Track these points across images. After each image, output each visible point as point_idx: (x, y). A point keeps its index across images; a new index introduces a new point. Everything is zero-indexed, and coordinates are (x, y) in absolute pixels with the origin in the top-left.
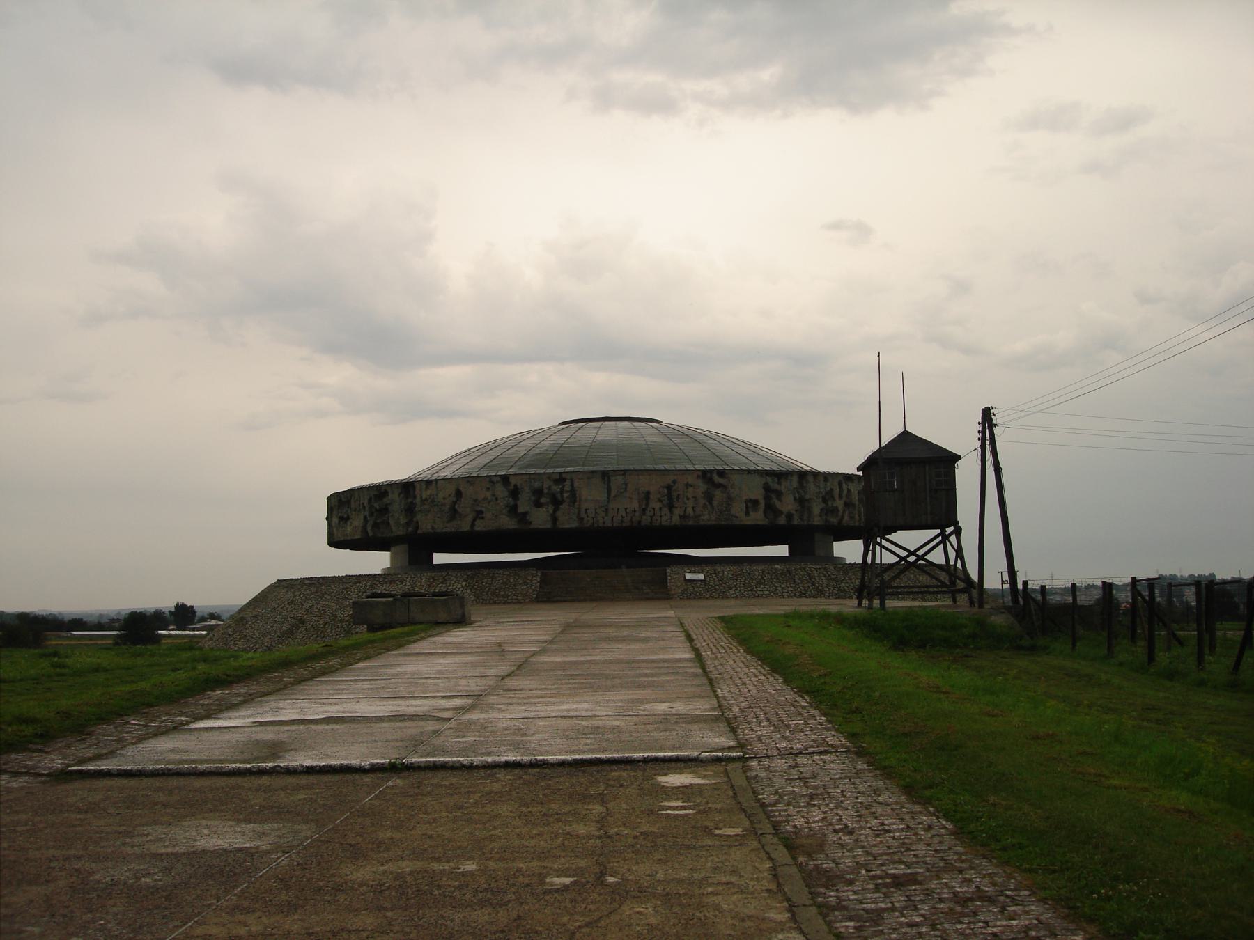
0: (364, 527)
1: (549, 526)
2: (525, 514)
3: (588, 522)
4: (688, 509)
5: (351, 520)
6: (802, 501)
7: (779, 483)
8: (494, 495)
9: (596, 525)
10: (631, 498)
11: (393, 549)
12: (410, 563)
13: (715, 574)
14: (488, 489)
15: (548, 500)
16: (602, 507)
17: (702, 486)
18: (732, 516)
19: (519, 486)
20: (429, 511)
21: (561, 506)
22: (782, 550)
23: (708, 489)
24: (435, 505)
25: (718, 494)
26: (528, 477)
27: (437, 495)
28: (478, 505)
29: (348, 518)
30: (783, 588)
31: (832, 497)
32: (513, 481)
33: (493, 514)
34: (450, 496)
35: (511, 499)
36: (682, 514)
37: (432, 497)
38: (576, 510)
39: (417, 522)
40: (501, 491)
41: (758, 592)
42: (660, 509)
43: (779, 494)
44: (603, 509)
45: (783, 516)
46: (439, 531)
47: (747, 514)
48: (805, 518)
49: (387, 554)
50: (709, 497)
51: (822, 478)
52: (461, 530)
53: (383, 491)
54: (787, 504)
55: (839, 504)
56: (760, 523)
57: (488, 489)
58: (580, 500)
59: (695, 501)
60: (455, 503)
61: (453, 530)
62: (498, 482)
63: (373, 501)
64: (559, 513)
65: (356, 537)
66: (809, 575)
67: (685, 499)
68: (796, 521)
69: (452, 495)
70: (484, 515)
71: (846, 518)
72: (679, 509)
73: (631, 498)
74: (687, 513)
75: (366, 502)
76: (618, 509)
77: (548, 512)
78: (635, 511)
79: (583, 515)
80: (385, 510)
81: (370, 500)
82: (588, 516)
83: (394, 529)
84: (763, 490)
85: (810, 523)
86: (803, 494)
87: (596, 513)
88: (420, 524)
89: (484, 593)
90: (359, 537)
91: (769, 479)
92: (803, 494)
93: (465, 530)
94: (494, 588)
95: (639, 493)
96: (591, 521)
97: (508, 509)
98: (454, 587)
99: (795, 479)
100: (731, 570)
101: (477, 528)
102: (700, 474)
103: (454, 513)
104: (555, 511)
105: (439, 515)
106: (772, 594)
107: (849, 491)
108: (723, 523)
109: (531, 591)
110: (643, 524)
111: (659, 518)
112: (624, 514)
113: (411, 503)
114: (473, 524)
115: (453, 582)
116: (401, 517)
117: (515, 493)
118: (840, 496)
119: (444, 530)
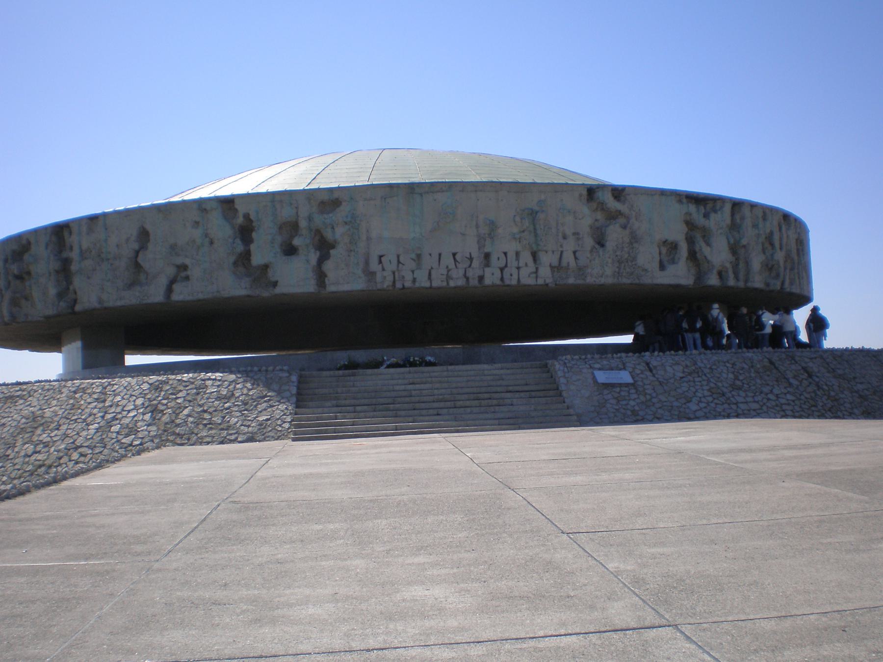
2: (266, 267)
3: (384, 281)
4: (565, 255)
6: (734, 249)
7: (706, 216)
8: (206, 235)
10: (463, 235)
13: (651, 370)
14: (197, 223)
17: (587, 217)
19: (252, 217)
20: (94, 270)
21: (332, 252)
27: (106, 241)
30: (777, 396)
31: (772, 245)
32: (241, 209)
34: (128, 240)
35: (238, 241)
36: (555, 263)
41: (741, 405)
42: (517, 254)
44: (413, 256)
45: (715, 272)
46: (111, 304)
47: (662, 267)
48: (742, 275)
49: (61, 354)
51: (760, 214)
52: (149, 301)
53: (24, 242)
55: (780, 256)
56: (683, 282)
57: (197, 224)
58: (369, 239)
59: (578, 239)
64: (328, 266)
66: (805, 369)
68: (731, 282)
70: (189, 273)
73: (463, 235)
76: (440, 255)
77: (308, 261)
78: (471, 259)
79: (374, 266)
82: (383, 270)
84: (684, 225)
85: (749, 284)
87: (399, 262)
91: (692, 208)
95: (477, 226)
96: (390, 278)
99: (728, 208)
100: (677, 364)
101: (176, 297)
102: (585, 193)
104: (321, 260)
106: (765, 408)
107: (788, 236)
110: (488, 281)
111: (515, 272)
112: (452, 265)
114: (169, 290)
118: (781, 249)
119: (119, 303)
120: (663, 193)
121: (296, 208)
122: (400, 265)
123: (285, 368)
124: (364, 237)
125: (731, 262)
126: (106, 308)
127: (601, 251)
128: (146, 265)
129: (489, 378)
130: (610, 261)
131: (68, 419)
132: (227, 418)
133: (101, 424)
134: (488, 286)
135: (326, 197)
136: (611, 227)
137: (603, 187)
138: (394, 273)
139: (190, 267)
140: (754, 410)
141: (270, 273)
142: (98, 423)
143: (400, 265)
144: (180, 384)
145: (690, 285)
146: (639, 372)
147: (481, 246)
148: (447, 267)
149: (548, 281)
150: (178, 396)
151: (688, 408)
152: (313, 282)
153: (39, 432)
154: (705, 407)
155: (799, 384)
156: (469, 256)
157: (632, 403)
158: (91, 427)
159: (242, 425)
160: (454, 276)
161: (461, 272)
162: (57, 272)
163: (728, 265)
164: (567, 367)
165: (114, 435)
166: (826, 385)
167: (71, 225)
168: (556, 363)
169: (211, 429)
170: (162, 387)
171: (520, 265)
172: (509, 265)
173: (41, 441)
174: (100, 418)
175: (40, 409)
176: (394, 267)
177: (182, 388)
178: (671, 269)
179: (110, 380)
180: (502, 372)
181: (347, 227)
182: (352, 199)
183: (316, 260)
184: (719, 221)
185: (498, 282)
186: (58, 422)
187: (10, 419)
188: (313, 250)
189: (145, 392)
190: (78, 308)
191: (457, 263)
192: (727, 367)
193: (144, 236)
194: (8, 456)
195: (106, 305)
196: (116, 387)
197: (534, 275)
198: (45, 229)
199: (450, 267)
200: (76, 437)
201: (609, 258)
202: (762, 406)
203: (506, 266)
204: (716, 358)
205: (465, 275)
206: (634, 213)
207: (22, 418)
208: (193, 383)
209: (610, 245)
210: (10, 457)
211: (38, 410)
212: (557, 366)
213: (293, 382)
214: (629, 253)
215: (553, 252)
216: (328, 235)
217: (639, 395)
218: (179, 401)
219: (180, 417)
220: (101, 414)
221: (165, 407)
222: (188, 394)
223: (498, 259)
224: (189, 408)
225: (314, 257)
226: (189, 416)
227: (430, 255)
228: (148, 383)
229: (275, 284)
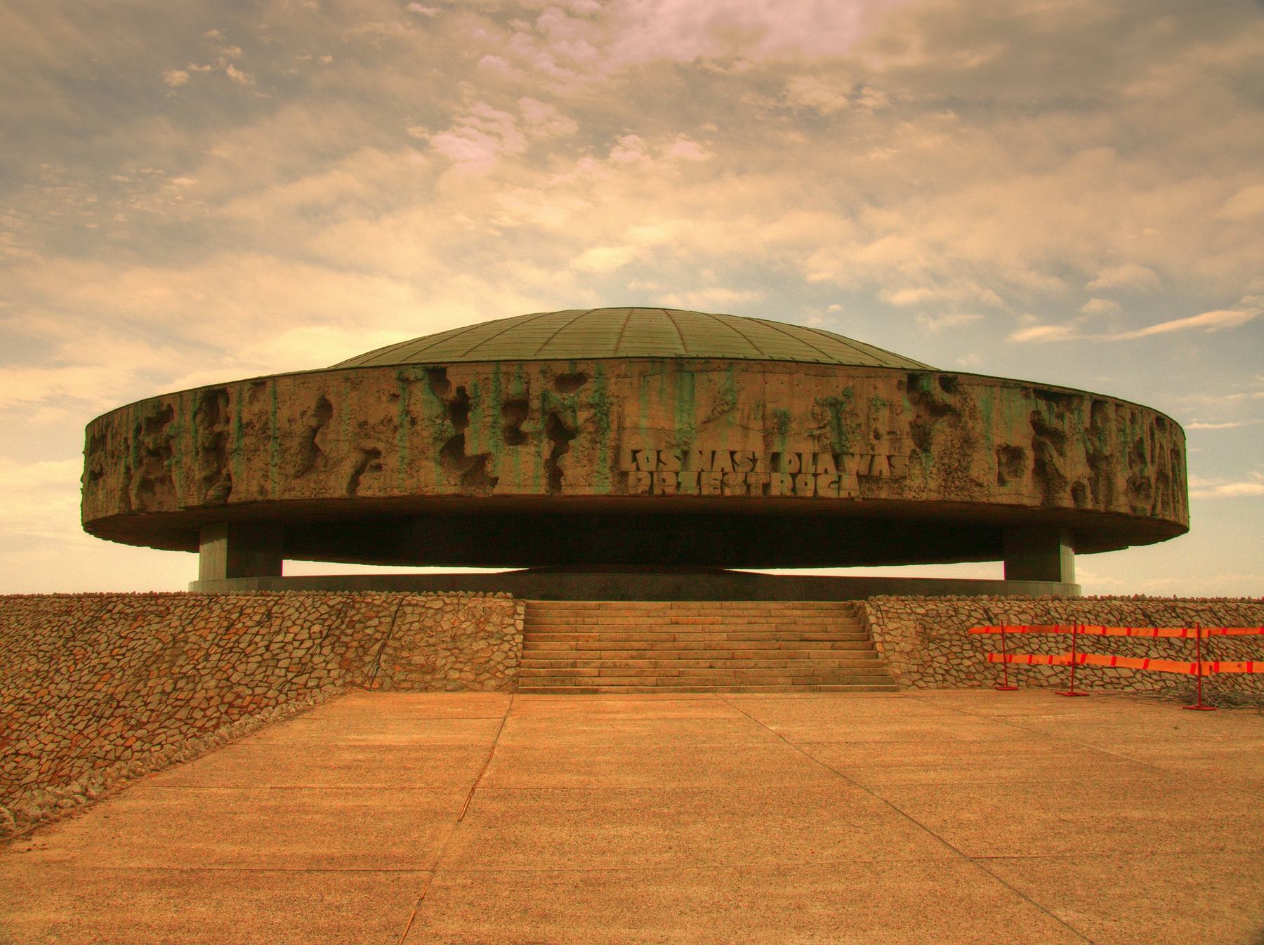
0: (125, 489)
1: (539, 488)
2: (482, 459)
3: (638, 484)
4: (877, 459)
5: (104, 477)
6: (1093, 460)
7: (1060, 417)
8: (408, 413)
9: (657, 491)
11: (201, 547)
12: (231, 573)
15: (540, 426)
16: (672, 446)
17: (908, 414)
18: (972, 480)
19: (468, 393)
20: (257, 450)
21: (571, 442)
22: (993, 570)
23: (918, 416)
24: (269, 437)
25: (942, 432)
26: (492, 368)
28: (368, 436)
29: (101, 474)
32: (455, 379)
33: (403, 458)
34: (304, 413)
35: (448, 422)
37: (264, 418)
38: (610, 454)
39: (229, 477)
40: (425, 403)
42: (815, 456)
43: (1058, 438)
44: (678, 453)
45: (1068, 489)
46: (275, 496)
47: (1002, 481)
49: (197, 556)
50: (923, 440)
51: (1128, 417)
53: (164, 408)
54: (1073, 466)
55: (1151, 471)
56: (1026, 501)
57: (395, 397)
58: (621, 428)
60: (314, 431)
61: (307, 494)
62: (417, 380)
63: (142, 433)
64: (567, 461)
65: (110, 513)
67: (871, 437)
68: (1089, 505)
69: (310, 412)
70: (382, 461)
71: (1159, 505)
72: (857, 458)
73: (746, 428)
74: (875, 472)
75: (131, 435)
76: (714, 453)
77: (539, 454)
78: (754, 460)
79: (627, 464)
80: (162, 452)
81: (138, 430)
82: (638, 469)
83: (179, 492)
85: (1112, 508)
86: (1097, 443)
87: (659, 460)
88: (234, 479)
89: (367, 659)
90: (116, 511)
91: (1042, 405)
92: (1097, 443)
93: (336, 495)
94: (397, 644)
95: (764, 418)
96: (648, 482)
97: (440, 445)
98: (290, 637)
99: (1087, 406)
100: (1023, 612)
101: (363, 492)
102: (905, 379)
103: (312, 456)
104: (555, 455)
105: (277, 460)
106: (1138, 676)
107: (1161, 446)
108: (953, 497)
109: (498, 656)
110: (775, 491)
111: (811, 480)
112: (728, 468)
113: (220, 434)
114: (354, 482)
115: (289, 623)
116: (196, 467)
117: (459, 409)
118: (1152, 462)
119: (287, 496)
120: (1005, 383)
121: (526, 383)
122: (661, 464)
123: (509, 594)
124: (614, 426)
125: (1089, 479)
126: (269, 501)
127: (923, 455)
128: (325, 448)
129: (777, 620)
130: (935, 471)
131: (219, 646)
132: (432, 659)
133: (265, 656)
134: (776, 497)
135: (566, 369)
136: (938, 426)
137: (926, 373)
138: (651, 473)
139: (384, 454)
140: (1126, 678)
141: (489, 467)
142: (261, 655)
143: (661, 464)
144: (370, 610)
145: (1036, 506)
146: (973, 621)
147: (767, 445)
148: (723, 470)
149: (853, 494)
150: (368, 624)
151: (1040, 672)
152: (544, 481)
153: (181, 661)
154: (1062, 672)
155: (1182, 645)
156: (751, 458)
157: (967, 662)
158: (251, 659)
159: (451, 668)
160: (731, 482)
161: (740, 478)
162: (206, 450)
163: (1085, 482)
164: (880, 611)
165: (283, 671)
166: (1219, 648)
167: (230, 390)
168: (867, 605)
169: (411, 671)
170: (346, 613)
171: (819, 472)
172: (803, 471)
173: (185, 674)
174: (263, 648)
175: (183, 631)
176: (652, 466)
177: (372, 614)
178: (1012, 483)
179: (276, 598)
180: (797, 612)
181: (593, 411)
182: (600, 374)
183: (550, 452)
184: (1075, 422)
185: (788, 493)
186: (208, 649)
187: (142, 642)
188: (546, 440)
189: (324, 617)
190: (232, 498)
191: (735, 465)
192: (1089, 619)
193: (324, 408)
194: (139, 691)
195: (271, 497)
196: (284, 608)
197: (836, 485)
198: (195, 391)
199: (726, 470)
200: (231, 671)
201: (934, 466)
202: (1135, 673)
203: (800, 471)
204: (1075, 607)
205: (745, 481)
206: (967, 409)
207: (157, 643)
208: (386, 609)
209: (935, 450)
210: (141, 693)
211: (180, 633)
212: (869, 610)
213: (520, 614)
214: (959, 461)
215: (862, 455)
216: (568, 419)
217: (975, 652)
218: (369, 631)
219: (369, 653)
220: (265, 643)
221: (350, 638)
222: (380, 623)
223: (790, 462)
224: (381, 642)
225: (546, 448)
226: (380, 652)
227: (701, 452)
228: (328, 605)
229: (495, 481)
